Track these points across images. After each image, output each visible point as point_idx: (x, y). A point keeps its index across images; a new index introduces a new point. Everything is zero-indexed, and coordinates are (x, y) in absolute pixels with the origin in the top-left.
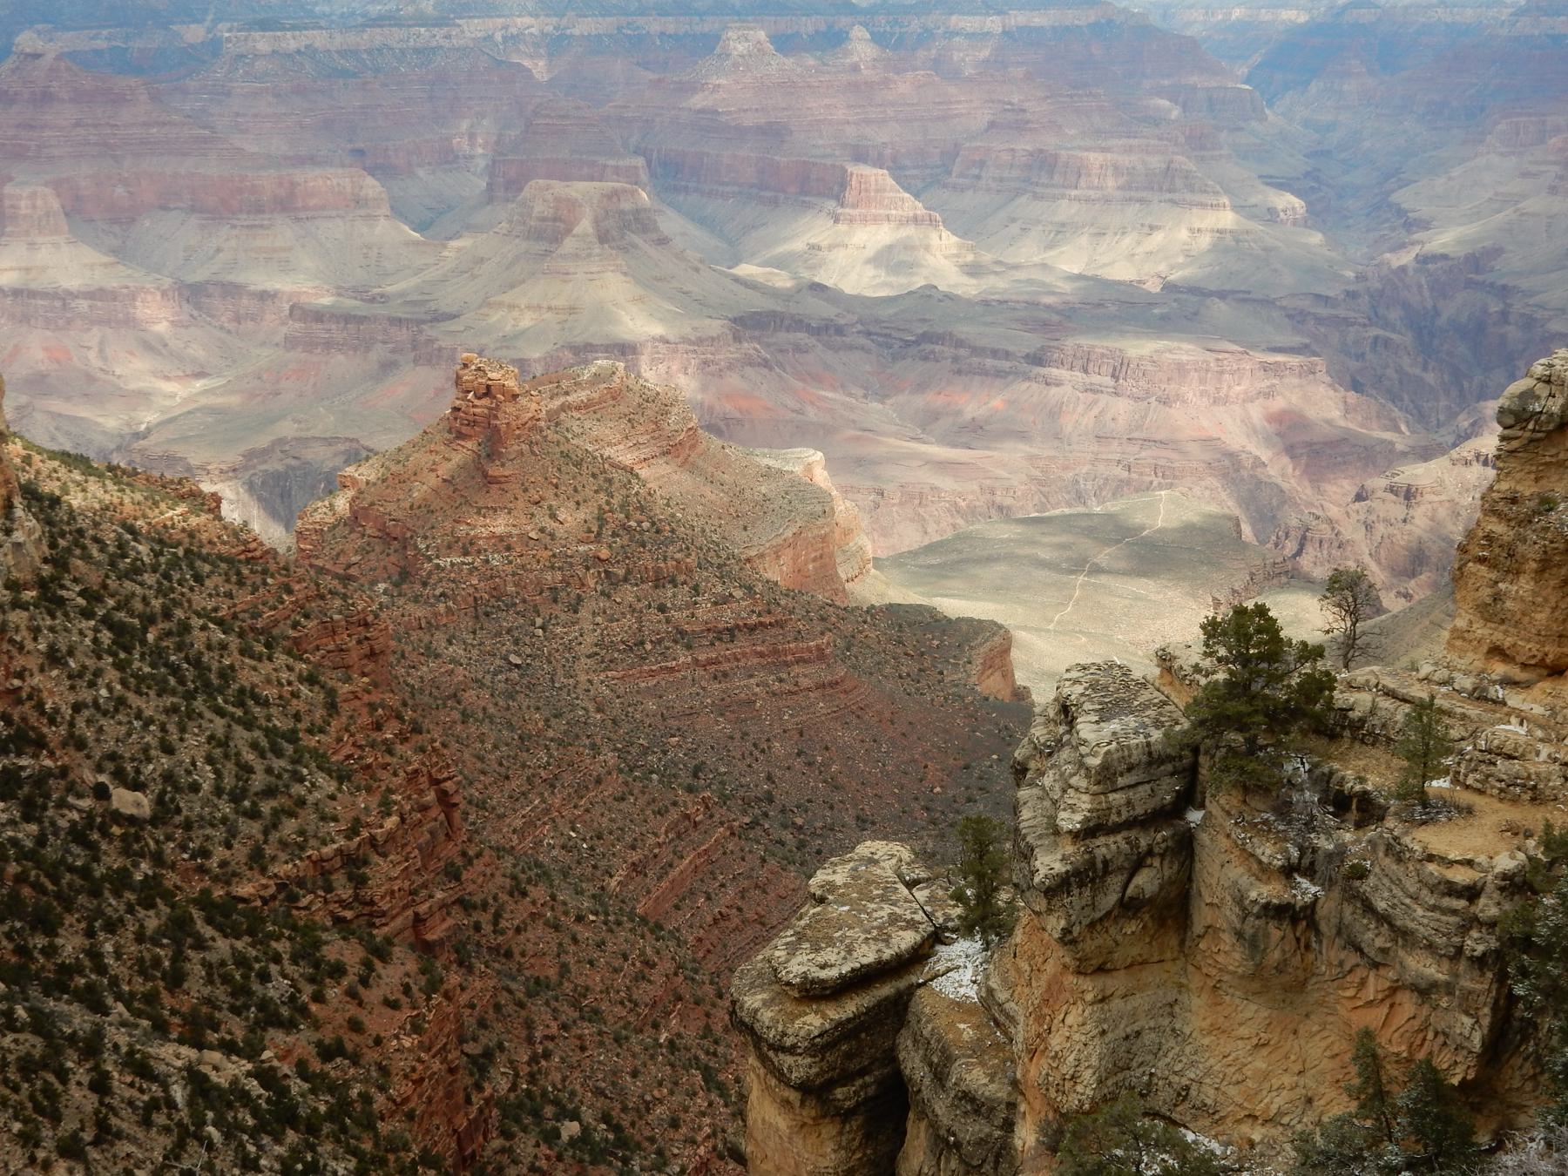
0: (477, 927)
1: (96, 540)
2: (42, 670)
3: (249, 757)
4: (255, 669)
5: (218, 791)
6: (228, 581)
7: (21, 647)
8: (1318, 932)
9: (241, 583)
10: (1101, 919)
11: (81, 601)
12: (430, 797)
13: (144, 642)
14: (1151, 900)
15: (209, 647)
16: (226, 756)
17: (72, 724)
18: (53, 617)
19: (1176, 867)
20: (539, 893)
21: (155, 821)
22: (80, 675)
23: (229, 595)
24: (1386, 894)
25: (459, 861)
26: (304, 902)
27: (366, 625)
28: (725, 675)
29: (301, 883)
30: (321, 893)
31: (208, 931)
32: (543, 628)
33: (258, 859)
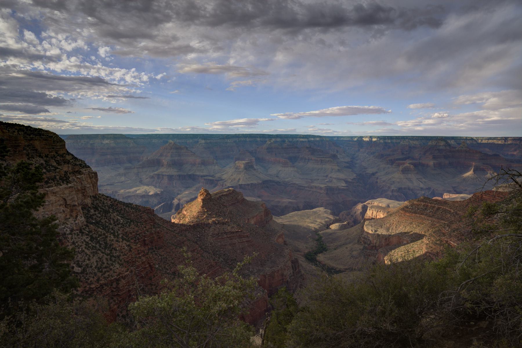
0: (152, 289)
5: (96, 267)
7: (68, 241)
16: (100, 261)
21: (81, 273)
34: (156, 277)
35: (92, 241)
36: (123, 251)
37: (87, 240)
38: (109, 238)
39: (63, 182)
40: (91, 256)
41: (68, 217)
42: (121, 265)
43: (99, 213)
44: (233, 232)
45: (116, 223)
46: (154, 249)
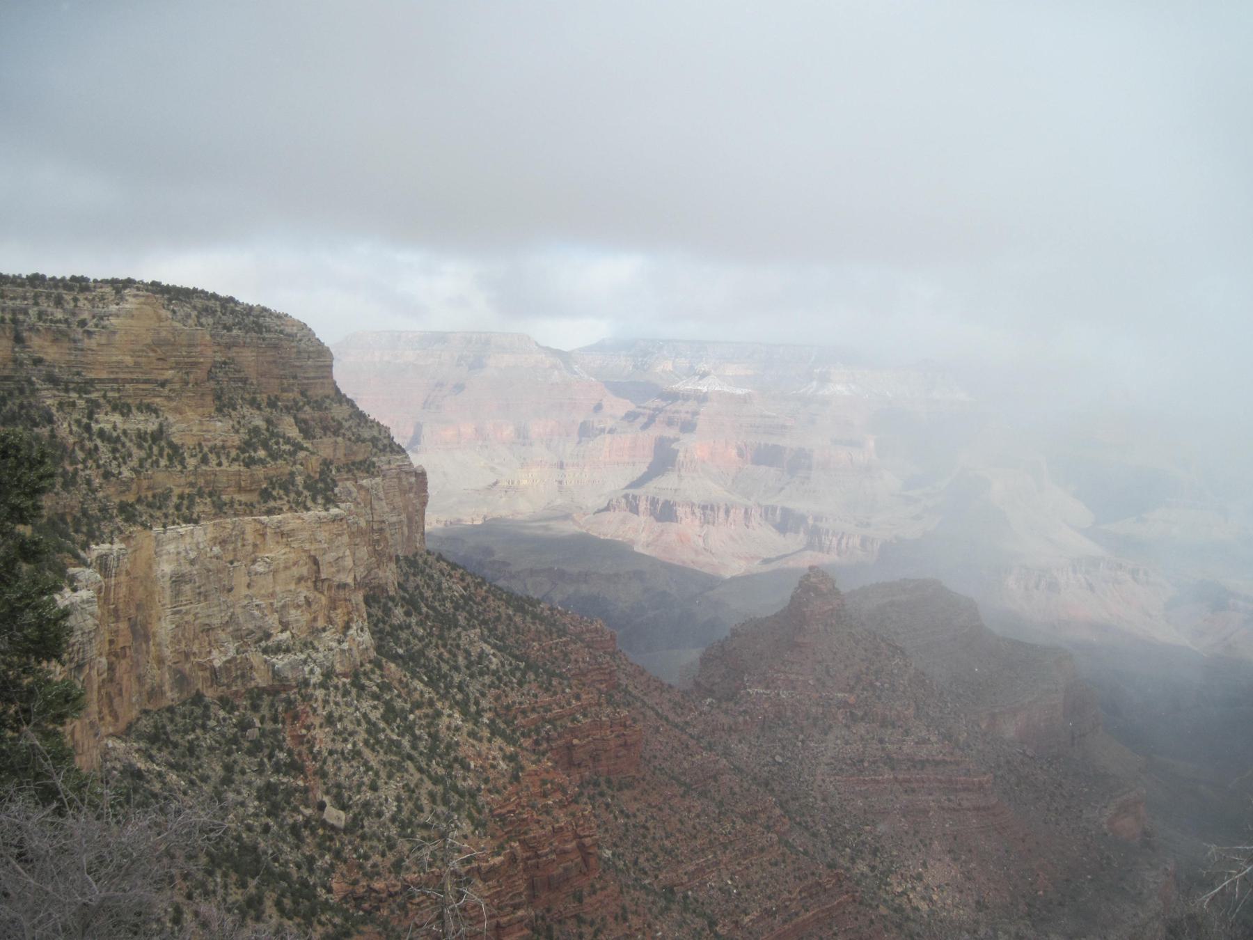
2: (321, 726)
3: (425, 801)
5: (393, 819)
6: (540, 687)
7: (315, 710)
11: (375, 688)
12: (570, 846)
13: (406, 718)
15: (448, 728)
16: (410, 798)
17: (325, 762)
20: (635, 921)
21: (346, 830)
22: (340, 733)
23: (535, 696)
27: (625, 726)
28: (913, 791)
32: (803, 741)
33: (397, 866)
34: (600, 895)
35: (387, 722)
36: (492, 774)
37: (375, 715)
38: (445, 720)
39: (314, 500)
40: (383, 774)
41: (320, 623)
42: (477, 824)
43: (421, 624)
44: (923, 764)
45: (477, 665)
46: (604, 787)
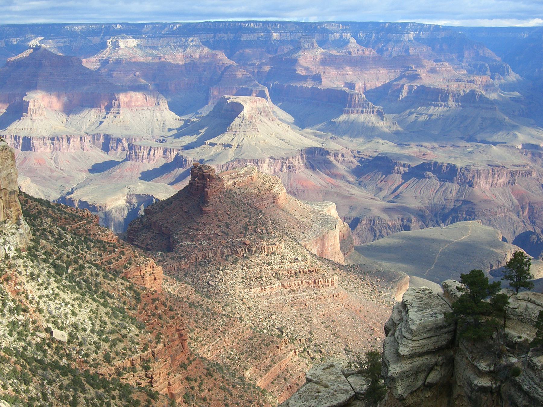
1: (50, 232)
3: (106, 319)
4: (109, 284)
5: (92, 331)
6: (100, 250)
8: (501, 398)
9: (105, 251)
10: (416, 391)
11: (44, 256)
12: (176, 336)
13: (67, 272)
14: (436, 384)
15: (92, 275)
17: (38, 303)
18: (33, 261)
19: (447, 370)
21: (69, 342)
24: (527, 383)
25: (186, 362)
26: (125, 376)
28: (294, 291)
29: (124, 369)
30: (131, 373)
31: (87, 386)
